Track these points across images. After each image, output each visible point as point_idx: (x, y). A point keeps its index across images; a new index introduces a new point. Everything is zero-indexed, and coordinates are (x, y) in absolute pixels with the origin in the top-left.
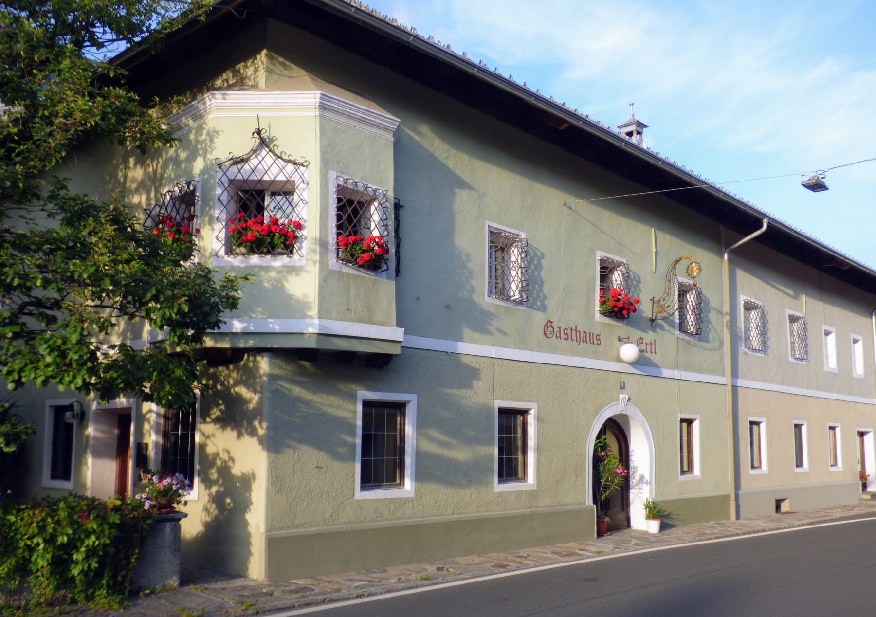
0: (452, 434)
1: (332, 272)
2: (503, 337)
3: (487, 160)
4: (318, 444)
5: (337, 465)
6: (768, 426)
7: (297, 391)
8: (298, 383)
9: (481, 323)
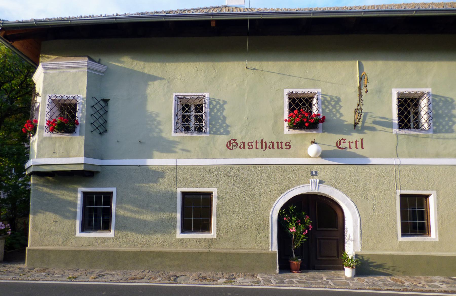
0: (142, 207)
1: (45, 138)
2: (187, 152)
3: (221, 61)
4: (55, 212)
5: (66, 221)
6: (438, 197)
7: (45, 189)
8: (46, 186)
9: (168, 148)
